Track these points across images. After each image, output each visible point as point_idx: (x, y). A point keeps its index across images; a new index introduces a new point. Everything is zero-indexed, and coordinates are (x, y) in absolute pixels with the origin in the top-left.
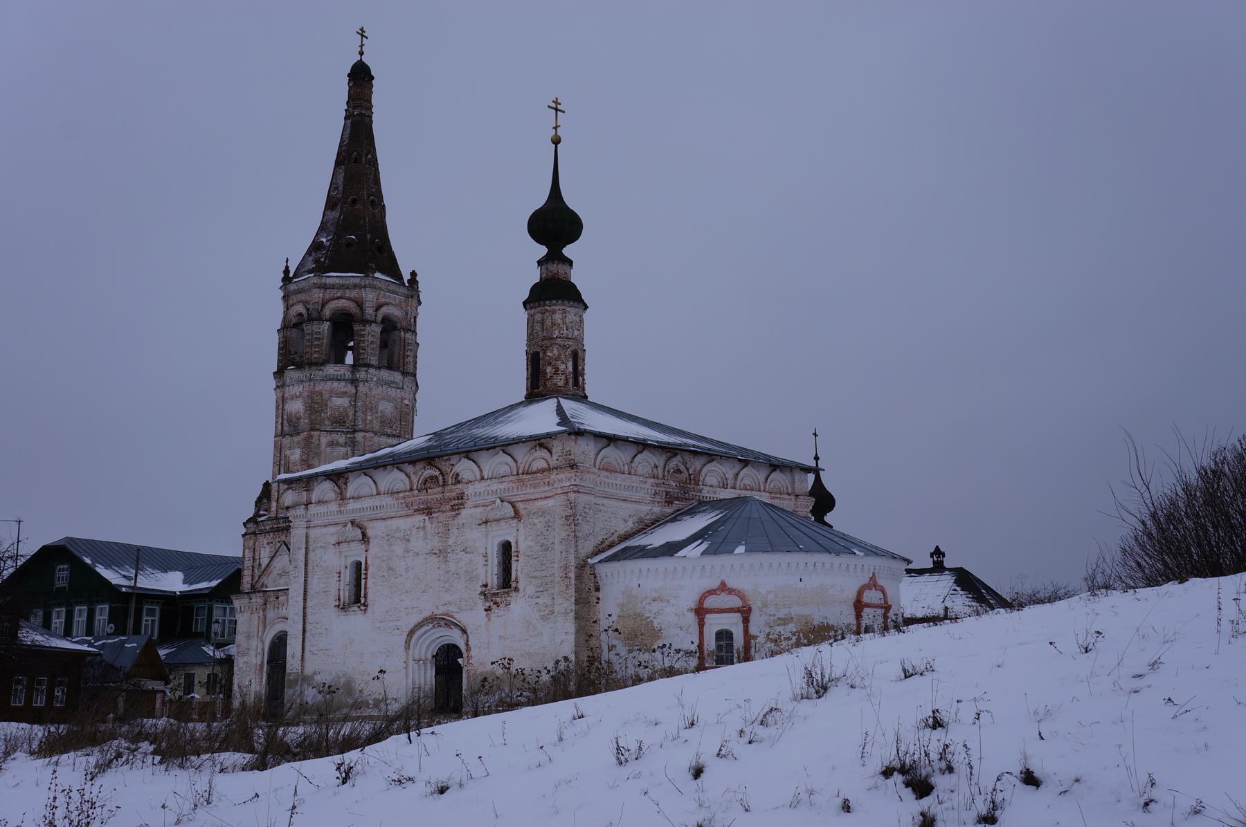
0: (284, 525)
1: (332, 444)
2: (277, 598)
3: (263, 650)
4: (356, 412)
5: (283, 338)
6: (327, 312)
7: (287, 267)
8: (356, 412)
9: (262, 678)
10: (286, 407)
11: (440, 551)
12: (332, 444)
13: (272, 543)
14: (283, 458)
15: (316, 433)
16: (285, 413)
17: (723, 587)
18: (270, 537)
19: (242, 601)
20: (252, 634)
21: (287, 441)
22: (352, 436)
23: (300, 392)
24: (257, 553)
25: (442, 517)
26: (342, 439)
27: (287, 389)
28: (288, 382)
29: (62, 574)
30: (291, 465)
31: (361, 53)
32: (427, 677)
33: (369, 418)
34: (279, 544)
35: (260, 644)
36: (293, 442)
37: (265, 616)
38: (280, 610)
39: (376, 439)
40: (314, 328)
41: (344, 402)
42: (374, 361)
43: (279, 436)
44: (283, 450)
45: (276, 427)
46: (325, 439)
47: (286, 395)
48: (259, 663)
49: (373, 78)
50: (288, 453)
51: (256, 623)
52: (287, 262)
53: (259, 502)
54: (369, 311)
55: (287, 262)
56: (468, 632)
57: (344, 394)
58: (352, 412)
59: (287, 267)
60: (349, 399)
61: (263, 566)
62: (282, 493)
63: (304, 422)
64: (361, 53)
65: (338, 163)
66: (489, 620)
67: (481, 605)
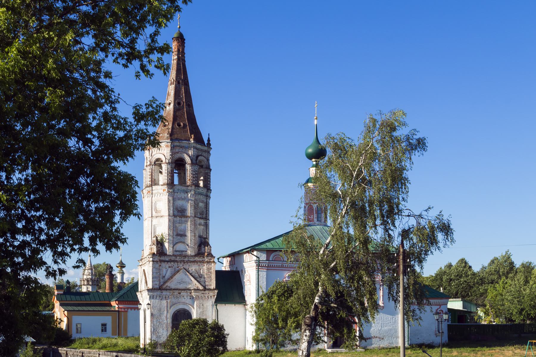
0: (180, 259)
2: (180, 293)
5: (171, 168)
13: (172, 267)
15: (196, 218)
22: (205, 221)
23: (185, 197)
27: (176, 194)
30: (178, 231)
36: (182, 221)
43: (172, 216)
45: (169, 212)
50: (177, 225)
57: (202, 202)
58: (205, 211)
60: (204, 204)
61: (166, 277)
62: (176, 244)
63: (189, 211)
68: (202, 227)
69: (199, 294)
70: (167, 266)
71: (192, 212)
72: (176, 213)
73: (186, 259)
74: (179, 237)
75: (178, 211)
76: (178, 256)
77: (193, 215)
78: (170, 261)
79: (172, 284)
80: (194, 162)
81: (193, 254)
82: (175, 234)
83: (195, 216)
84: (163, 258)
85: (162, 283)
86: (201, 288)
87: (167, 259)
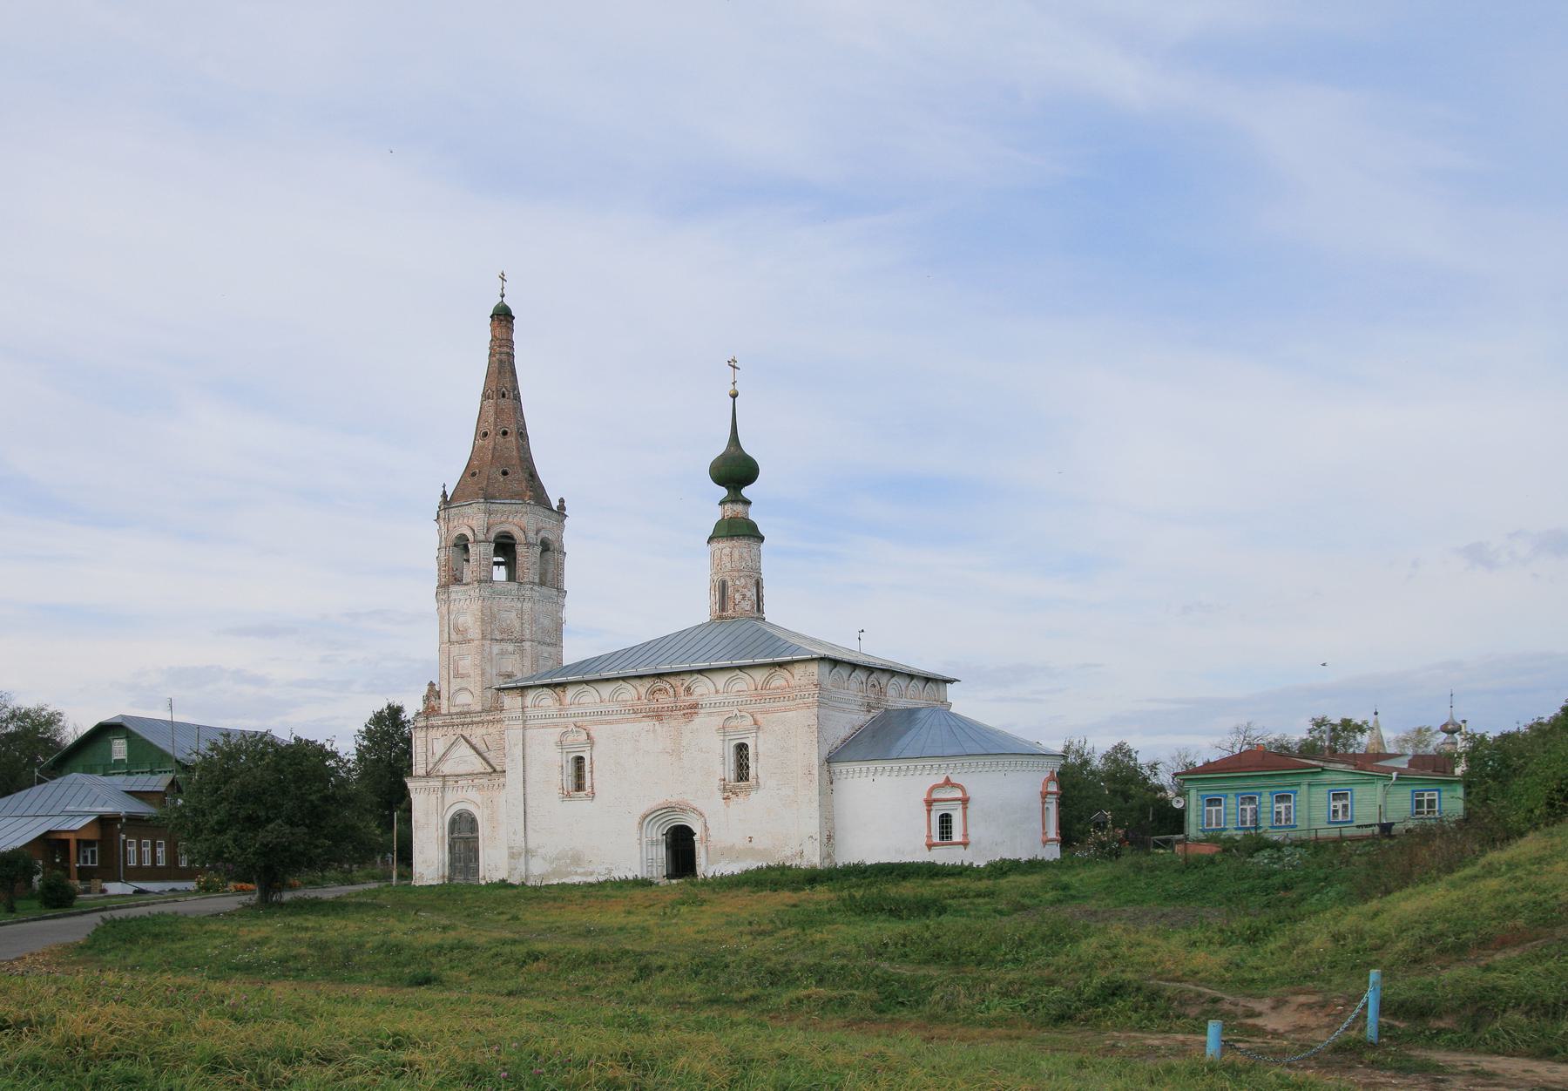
1: (503, 653)
2: (457, 782)
3: (443, 825)
4: (522, 624)
6: (492, 536)
7: (445, 492)
8: (522, 624)
9: (444, 848)
10: (452, 617)
11: (673, 751)
12: (503, 653)
14: (451, 662)
16: (451, 623)
17: (947, 782)
18: (441, 731)
19: (418, 784)
20: (430, 812)
21: (455, 649)
24: (430, 744)
25: (674, 723)
26: (510, 647)
28: (453, 596)
29: (119, 749)
31: (503, 296)
32: (661, 852)
33: (534, 629)
34: (455, 737)
35: (440, 820)
37: (443, 797)
38: (459, 792)
39: (540, 647)
40: (482, 549)
41: (513, 615)
42: (537, 581)
44: (451, 656)
46: (496, 648)
47: (452, 607)
48: (440, 835)
49: (514, 318)
51: (435, 802)
52: (444, 487)
53: (427, 698)
54: (531, 535)
55: (444, 487)
56: (706, 816)
59: (445, 492)
61: (437, 757)
63: (475, 632)
64: (503, 296)
65: (485, 396)
66: (728, 806)
67: (719, 795)
68: (511, 656)
69: (484, 781)
70: (439, 735)
71: (478, 631)
72: (454, 637)
73: (468, 720)
74: (459, 680)
75: (458, 631)
76: (457, 714)
77: (480, 637)
78: (444, 725)
79: (446, 768)
80: (481, 537)
81: (479, 708)
82: (452, 673)
83: (484, 638)
84: (434, 721)
85: (431, 766)
86: (490, 770)
87: (440, 722)
